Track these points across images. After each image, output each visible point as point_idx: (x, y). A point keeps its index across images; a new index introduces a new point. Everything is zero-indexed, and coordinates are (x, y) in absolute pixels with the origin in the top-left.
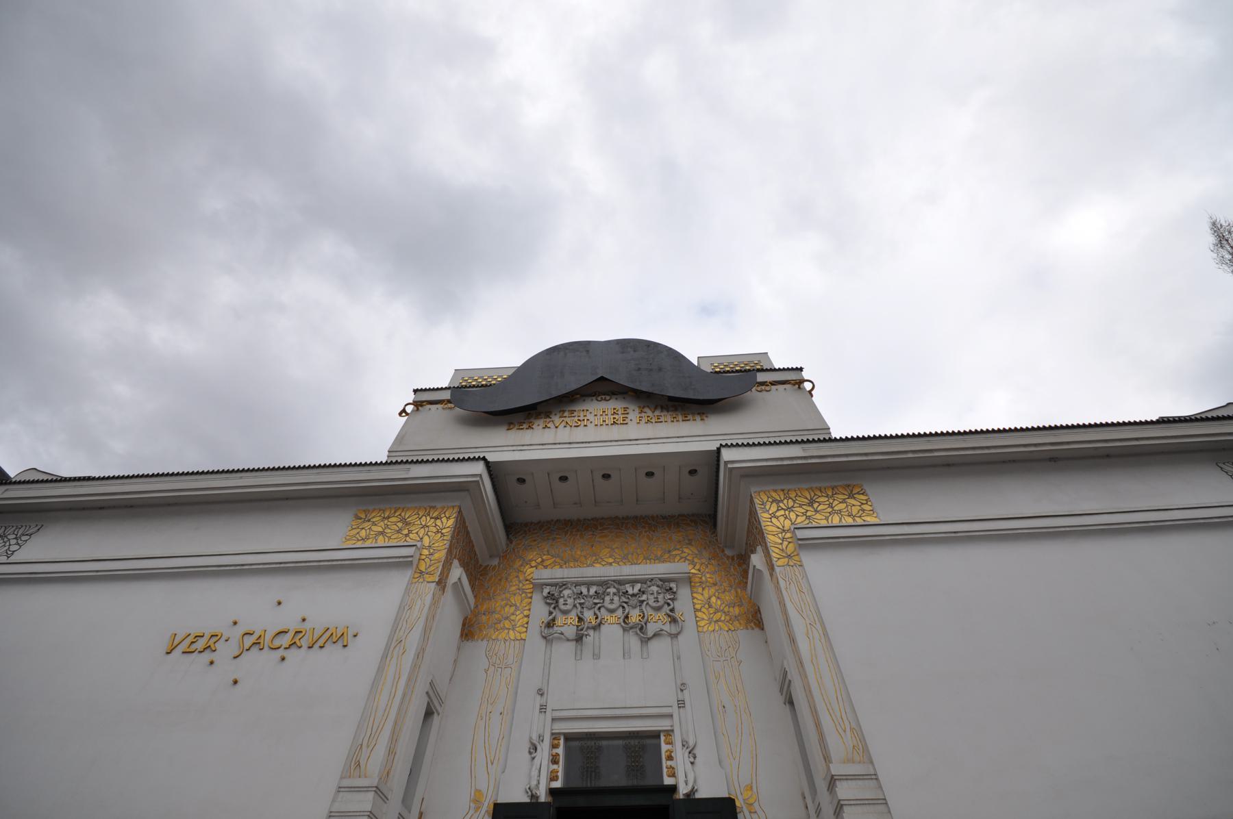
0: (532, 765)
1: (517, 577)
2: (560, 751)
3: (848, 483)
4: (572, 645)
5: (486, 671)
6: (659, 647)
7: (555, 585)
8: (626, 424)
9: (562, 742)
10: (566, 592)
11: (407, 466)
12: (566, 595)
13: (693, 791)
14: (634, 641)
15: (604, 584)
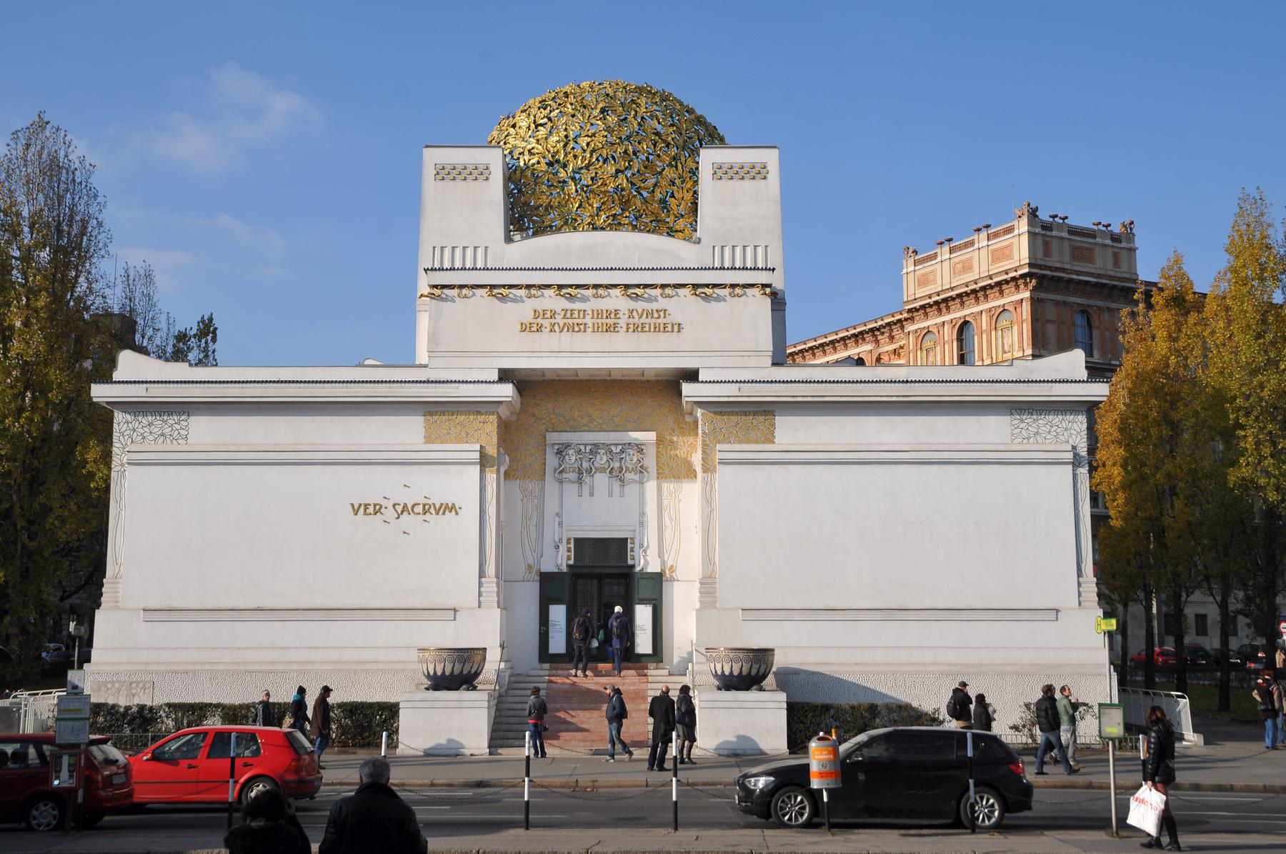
0: (558, 555)
1: (533, 432)
2: (572, 546)
3: (767, 409)
4: (576, 485)
5: (522, 500)
6: (631, 490)
7: (563, 444)
8: (618, 331)
9: (572, 541)
10: (571, 452)
11: (457, 385)
12: (570, 453)
13: (643, 569)
14: (616, 485)
15: (597, 446)
